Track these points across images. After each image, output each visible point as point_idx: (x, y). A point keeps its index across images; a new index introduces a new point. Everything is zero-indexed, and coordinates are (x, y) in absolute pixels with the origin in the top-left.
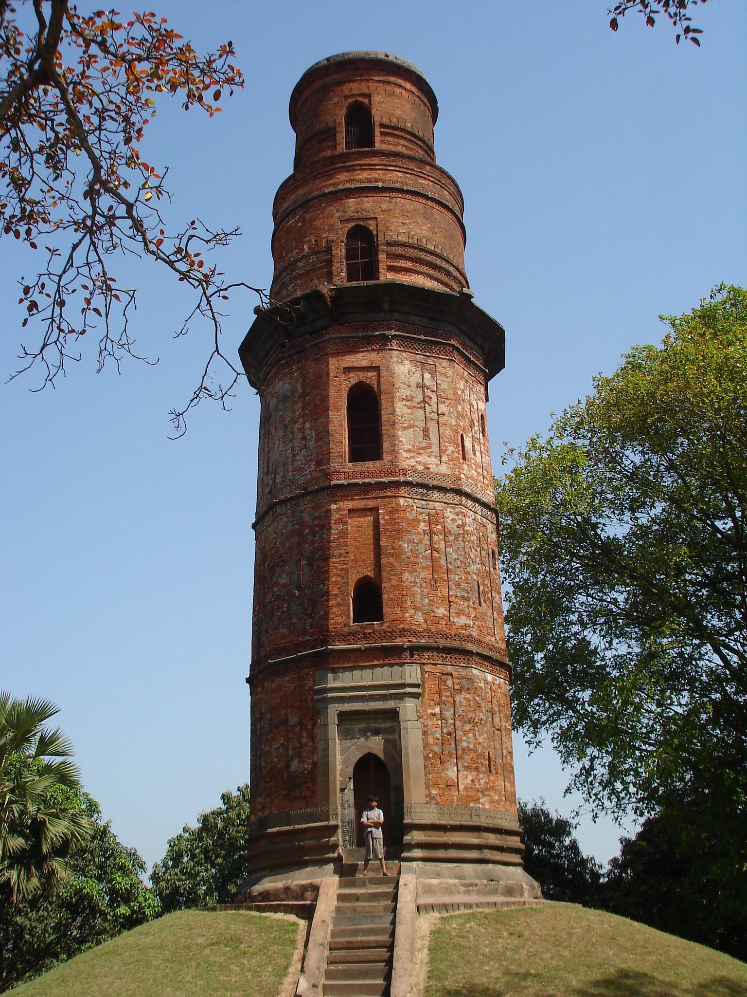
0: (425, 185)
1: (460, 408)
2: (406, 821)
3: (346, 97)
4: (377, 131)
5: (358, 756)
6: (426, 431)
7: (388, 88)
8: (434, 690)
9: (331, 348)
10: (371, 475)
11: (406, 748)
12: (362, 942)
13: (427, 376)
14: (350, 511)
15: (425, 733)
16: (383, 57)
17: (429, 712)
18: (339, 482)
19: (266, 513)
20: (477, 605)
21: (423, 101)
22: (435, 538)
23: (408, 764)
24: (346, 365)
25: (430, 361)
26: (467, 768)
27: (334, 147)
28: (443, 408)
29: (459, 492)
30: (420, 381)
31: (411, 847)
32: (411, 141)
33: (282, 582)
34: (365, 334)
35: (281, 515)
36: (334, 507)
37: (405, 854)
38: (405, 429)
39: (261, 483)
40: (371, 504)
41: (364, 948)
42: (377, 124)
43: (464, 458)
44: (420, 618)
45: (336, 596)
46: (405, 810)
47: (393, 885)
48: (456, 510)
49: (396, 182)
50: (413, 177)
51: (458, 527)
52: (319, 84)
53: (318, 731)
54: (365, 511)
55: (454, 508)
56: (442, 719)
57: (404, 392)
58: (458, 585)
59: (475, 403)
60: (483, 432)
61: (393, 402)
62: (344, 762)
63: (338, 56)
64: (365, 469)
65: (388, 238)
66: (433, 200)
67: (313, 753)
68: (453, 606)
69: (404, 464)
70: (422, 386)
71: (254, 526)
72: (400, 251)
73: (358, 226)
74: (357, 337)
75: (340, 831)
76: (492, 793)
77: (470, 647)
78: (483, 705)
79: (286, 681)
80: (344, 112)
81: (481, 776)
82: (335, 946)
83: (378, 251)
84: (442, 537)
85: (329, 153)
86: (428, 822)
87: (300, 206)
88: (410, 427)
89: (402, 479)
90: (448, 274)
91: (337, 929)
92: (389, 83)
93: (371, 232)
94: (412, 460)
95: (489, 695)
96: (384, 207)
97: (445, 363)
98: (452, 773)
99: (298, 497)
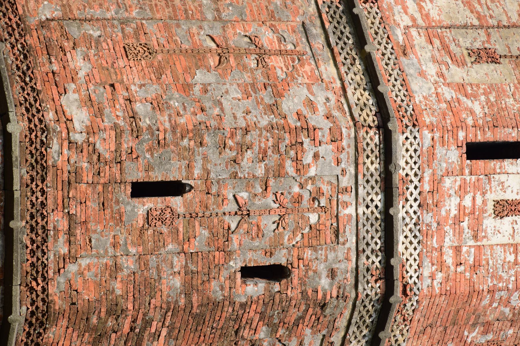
48: (336, 113)
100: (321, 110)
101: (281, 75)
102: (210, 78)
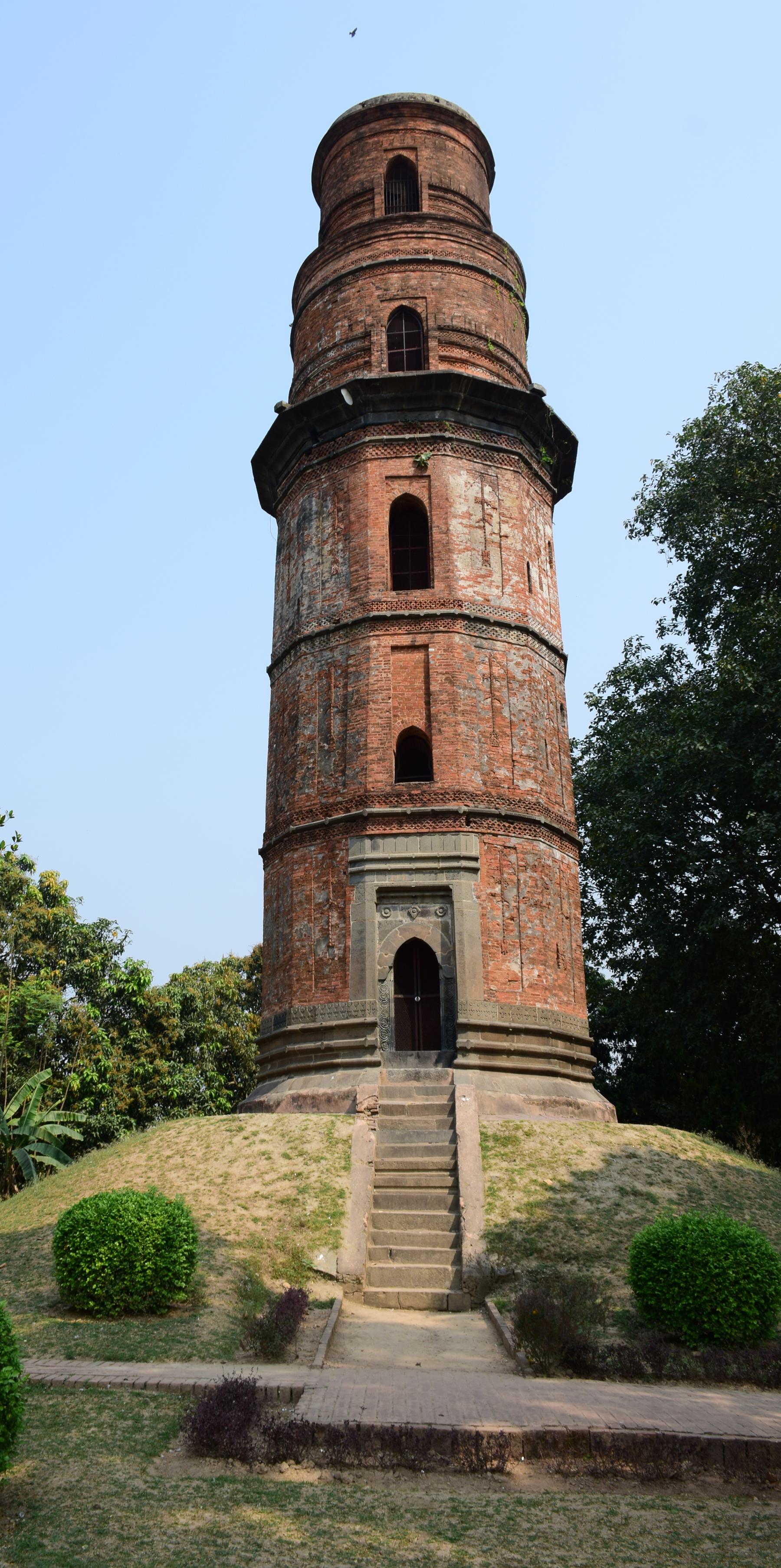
0: (484, 259)
1: (526, 530)
2: (461, 1019)
3: (386, 151)
4: (425, 193)
5: (400, 940)
6: (486, 557)
7: (438, 140)
8: (494, 866)
9: (370, 452)
10: (419, 605)
11: (461, 934)
12: (417, 1163)
13: (487, 489)
14: (395, 648)
15: (483, 915)
16: (432, 101)
17: (489, 891)
18: (380, 613)
19: (286, 653)
20: (544, 767)
21: (479, 161)
22: (497, 684)
23: (462, 951)
24: (390, 474)
25: (490, 472)
26: (533, 961)
27: (373, 211)
28: (506, 529)
29: (525, 631)
30: (480, 495)
31: (465, 1051)
32: (465, 208)
33: (307, 732)
34: (412, 436)
35: (305, 654)
36: (374, 643)
37: (460, 1060)
38: (460, 552)
39: (279, 619)
40: (421, 639)
41: (418, 1170)
42: (425, 185)
43: (530, 591)
44: (478, 779)
45: (376, 750)
46: (459, 1007)
47: (447, 1097)
48: (521, 653)
49: (450, 254)
50: (470, 250)
51: (524, 672)
52: (352, 135)
53: (351, 911)
54: (412, 648)
55: (519, 650)
56: (503, 900)
57: (460, 508)
58: (523, 742)
59: (541, 527)
60: (551, 562)
61: (446, 519)
62: (385, 947)
63: (376, 99)
64: (410, 598)
65: (440, 323)
66: (493, 277)
67: (344, 936)
68: (518, 766)
69: (460, 595)
70: (482, 502)
71: (270, 671)
72: (455, 337)
73: (402, 307)
74: (404, 439)
75: (378, 1029)
76: (561, 993)
77: (537, 816)
78: (551, 886)
79: (313, 851)
80: (382, 170)
81: (548, 971)
82: (382, 1167)
83: (427, 337)
84: (504, 683)
85: (366, 218)
86: (487, 1022)
87: (332, 283)
88: (467, 549)
89: (457, 611)
90: (511, 370)
91: (382, 1146)
92: (439, 134)
93: (418, 315)
94: (470, 589)
95: (557, 876)
96: (435, 284)
97: (509, 475)
98: (515, 968)
99: (326, 633)
100: (520, 660)
101: (502, 672)
102: (506, 709)
